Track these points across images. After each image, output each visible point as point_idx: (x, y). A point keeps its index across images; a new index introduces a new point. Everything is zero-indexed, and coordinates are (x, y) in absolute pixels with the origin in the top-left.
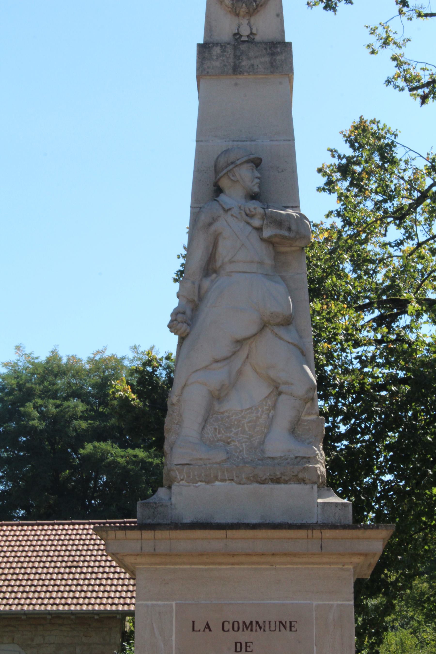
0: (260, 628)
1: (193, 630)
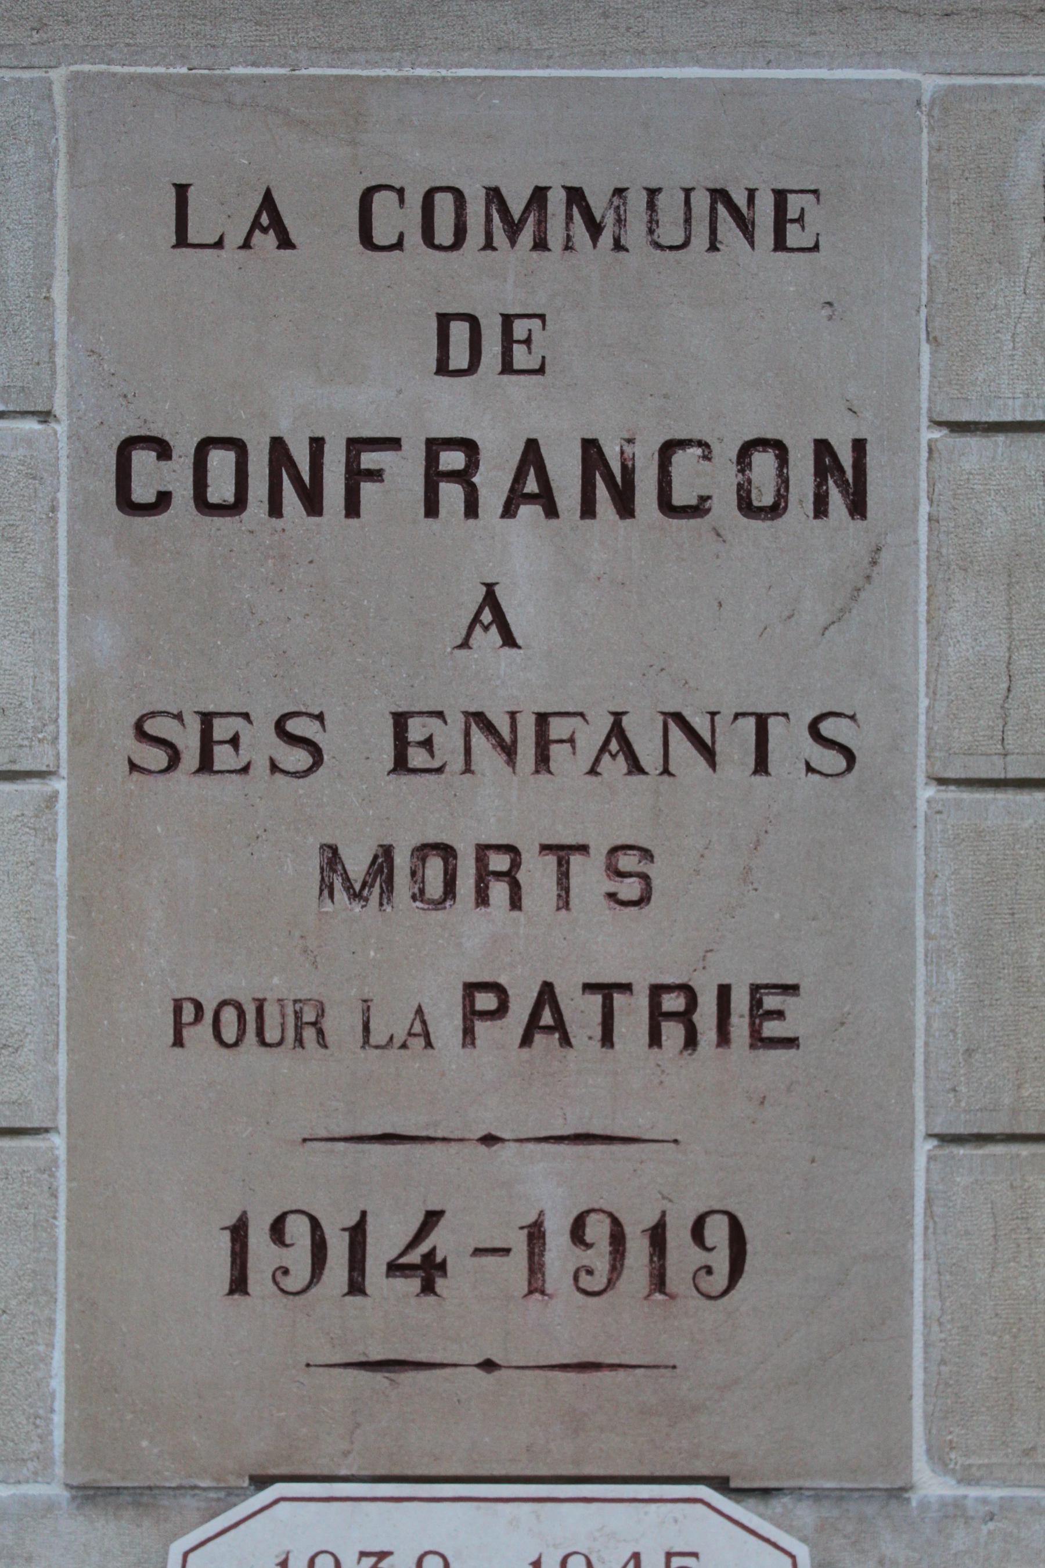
0: (595, 229)
1: (182, 240)
